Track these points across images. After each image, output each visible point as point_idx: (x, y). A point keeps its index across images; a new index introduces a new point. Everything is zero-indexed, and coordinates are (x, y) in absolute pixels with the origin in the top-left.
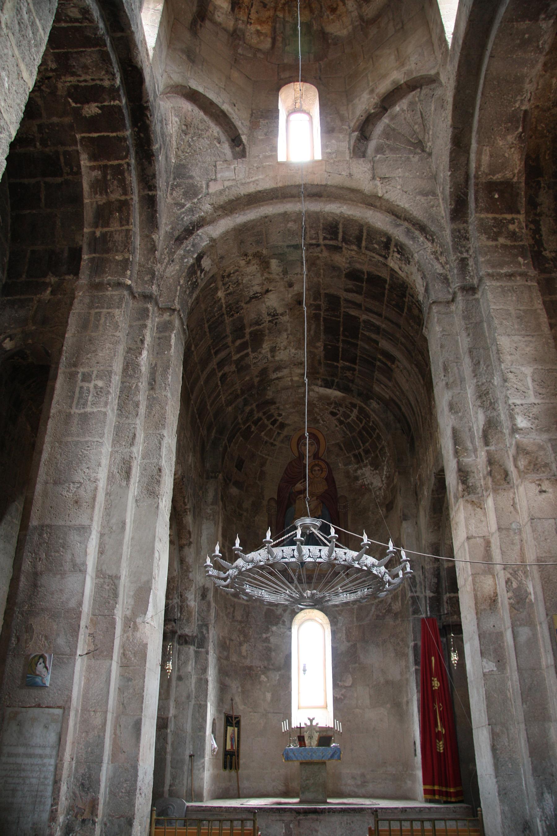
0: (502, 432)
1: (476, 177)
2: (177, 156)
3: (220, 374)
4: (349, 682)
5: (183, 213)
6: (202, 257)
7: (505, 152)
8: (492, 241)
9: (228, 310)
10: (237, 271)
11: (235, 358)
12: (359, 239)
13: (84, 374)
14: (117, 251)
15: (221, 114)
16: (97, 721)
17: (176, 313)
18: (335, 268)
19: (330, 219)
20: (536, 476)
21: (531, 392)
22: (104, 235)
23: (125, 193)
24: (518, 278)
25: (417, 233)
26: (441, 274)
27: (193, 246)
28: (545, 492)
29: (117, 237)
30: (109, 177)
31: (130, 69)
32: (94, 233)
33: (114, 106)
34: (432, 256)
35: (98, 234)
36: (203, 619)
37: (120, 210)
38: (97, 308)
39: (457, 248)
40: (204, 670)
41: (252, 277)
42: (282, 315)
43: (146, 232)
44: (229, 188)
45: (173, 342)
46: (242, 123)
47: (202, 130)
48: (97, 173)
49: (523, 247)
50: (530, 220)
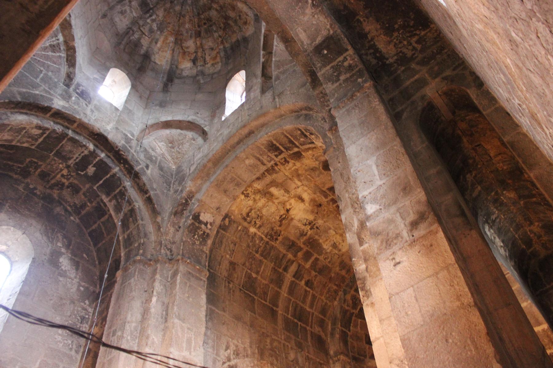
2: (175, 163)
3: (303, 283)
6: (199, 216)
7: (312, 21)
8: (336, 83)
9: (269, 237)
10: (251, 210)
11: (308, 265)
12: (291, 142)
15: (189, 124)
17: (180, 261)
18: (313, 169)
19: (265, 142)
20: (389, 252)
22: (128, 236)
28: (399, 263)
30: (119, 200)
31: (96, 137)
32: (124, 237)
33: (98, 161)
34: (322, 122)
35: (126, 237)
37: (131, 216)
39: (325, 105)
41: (267, 207)
42: (315, 220)
43: (154, 220)
44: (199, 164)
45: (178, 281)
46: (205, 121)
47: (182, 140)
48: (114, 202)
49: (360, 70)
50: (367, 48)
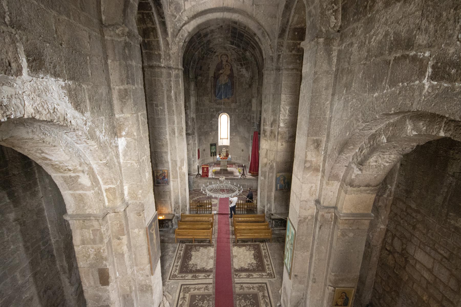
0: (276, 123)
1: (290, 26)
4: (234, 134)
5: (177, 21)
13: (155, 104)
14: (155, 50)
16: (177, 191)
21: (287, 115)
23: (153, 24)
24: (295, 70)
25: (266, 34)
26: (271, 56)
27: (182, 36)
29: (154, 43)
30: (145, 17)
36: (193, 127)
38: (154, 77)
40: (195, 141)
43: (164, 37)
44: (193, 6)
